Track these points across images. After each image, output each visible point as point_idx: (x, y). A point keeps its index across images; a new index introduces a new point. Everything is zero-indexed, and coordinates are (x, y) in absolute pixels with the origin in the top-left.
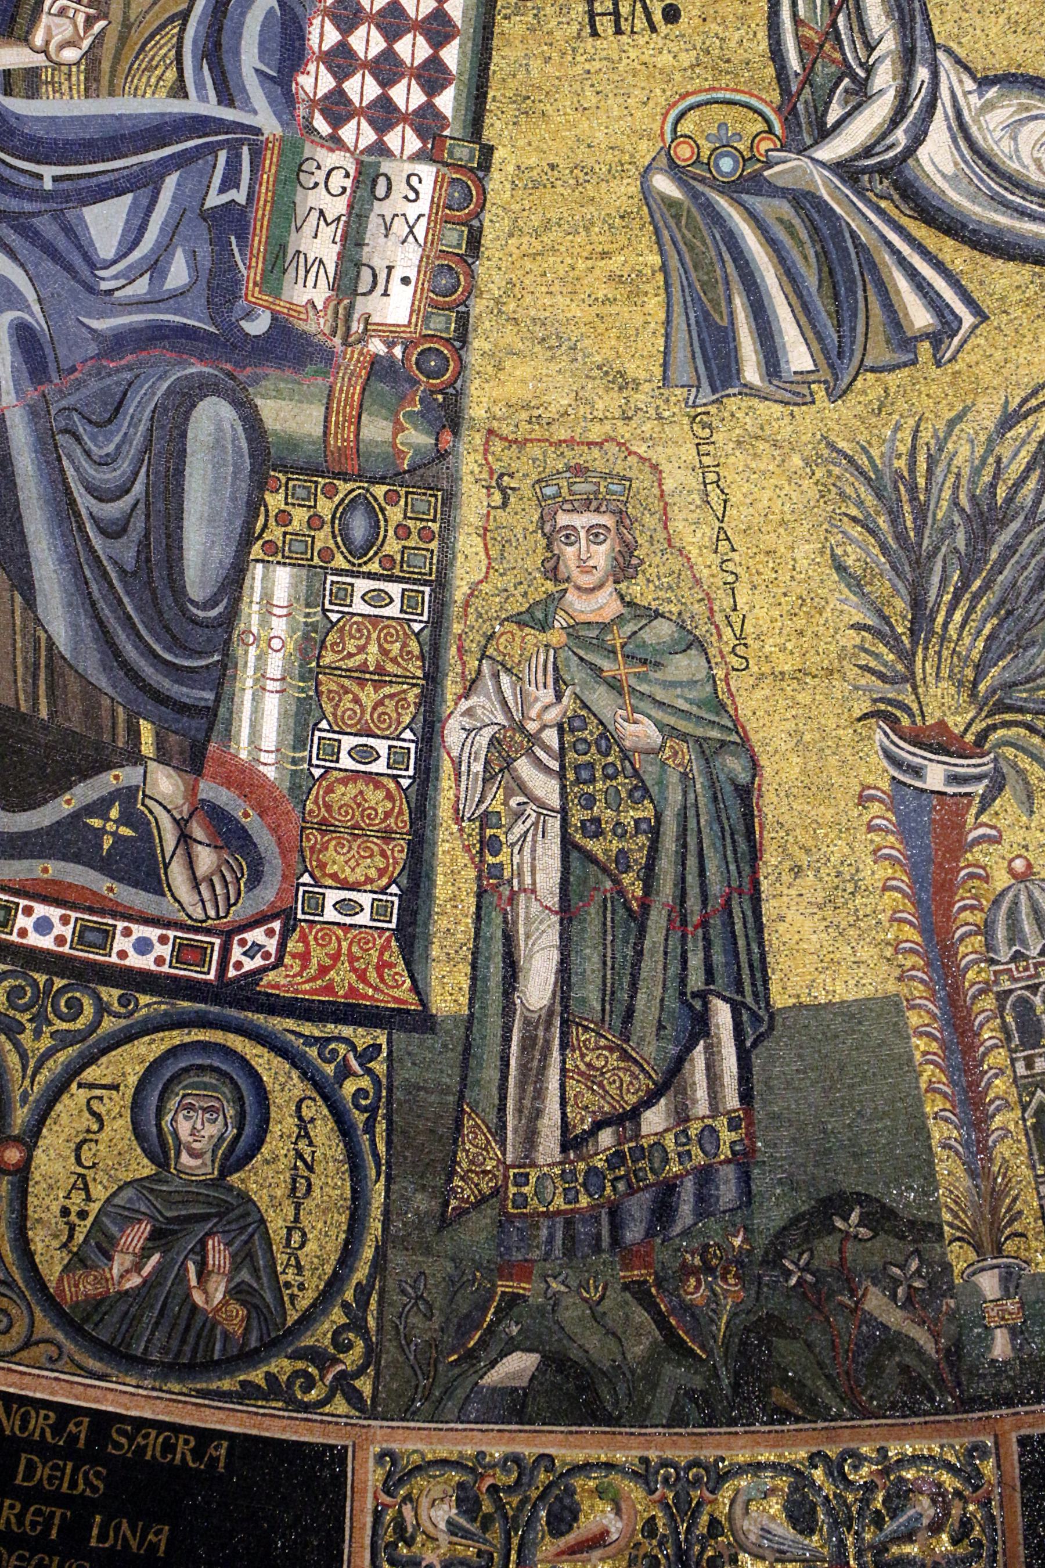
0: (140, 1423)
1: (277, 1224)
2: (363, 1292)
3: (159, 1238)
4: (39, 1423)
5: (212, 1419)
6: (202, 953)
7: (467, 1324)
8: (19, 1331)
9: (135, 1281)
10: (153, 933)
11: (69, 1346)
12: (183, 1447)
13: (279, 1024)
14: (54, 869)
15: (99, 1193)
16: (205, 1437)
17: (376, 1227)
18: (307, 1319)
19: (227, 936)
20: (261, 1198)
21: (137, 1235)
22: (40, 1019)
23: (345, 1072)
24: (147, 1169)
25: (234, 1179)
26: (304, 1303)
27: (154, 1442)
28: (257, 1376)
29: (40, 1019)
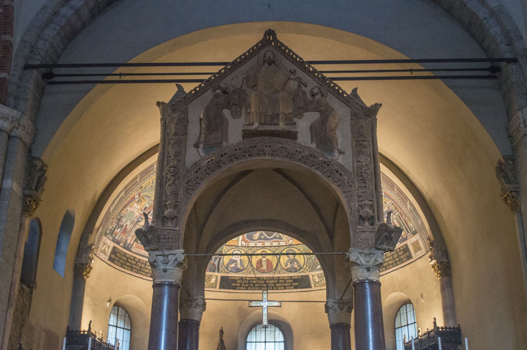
0: (294, 276)
1: (299, 260)
2: (307, 264)
3: (291, 263)
4: (287, 278)
5: (299, 275)
6: (287, 243)
7: (315, 264)
8: (283, 272)
9: (290, 266)
10: (283, 242)
11: (287, 272)
12: (297, 277)
13: (294, 246)
14: (274, 240)
15: (286, 261)
16: (298, 276)
17: (306, 259)
18: (303, 266)
19: (289, 241)
20: (297, 258)
21: (289, 263)
22: (277, 250)
23: (300, 249)
24: (288, 259)
25: (295, 258)
26: (303, 265)
27: (295, 277)
28: (301, 271)
29: (277, 250)
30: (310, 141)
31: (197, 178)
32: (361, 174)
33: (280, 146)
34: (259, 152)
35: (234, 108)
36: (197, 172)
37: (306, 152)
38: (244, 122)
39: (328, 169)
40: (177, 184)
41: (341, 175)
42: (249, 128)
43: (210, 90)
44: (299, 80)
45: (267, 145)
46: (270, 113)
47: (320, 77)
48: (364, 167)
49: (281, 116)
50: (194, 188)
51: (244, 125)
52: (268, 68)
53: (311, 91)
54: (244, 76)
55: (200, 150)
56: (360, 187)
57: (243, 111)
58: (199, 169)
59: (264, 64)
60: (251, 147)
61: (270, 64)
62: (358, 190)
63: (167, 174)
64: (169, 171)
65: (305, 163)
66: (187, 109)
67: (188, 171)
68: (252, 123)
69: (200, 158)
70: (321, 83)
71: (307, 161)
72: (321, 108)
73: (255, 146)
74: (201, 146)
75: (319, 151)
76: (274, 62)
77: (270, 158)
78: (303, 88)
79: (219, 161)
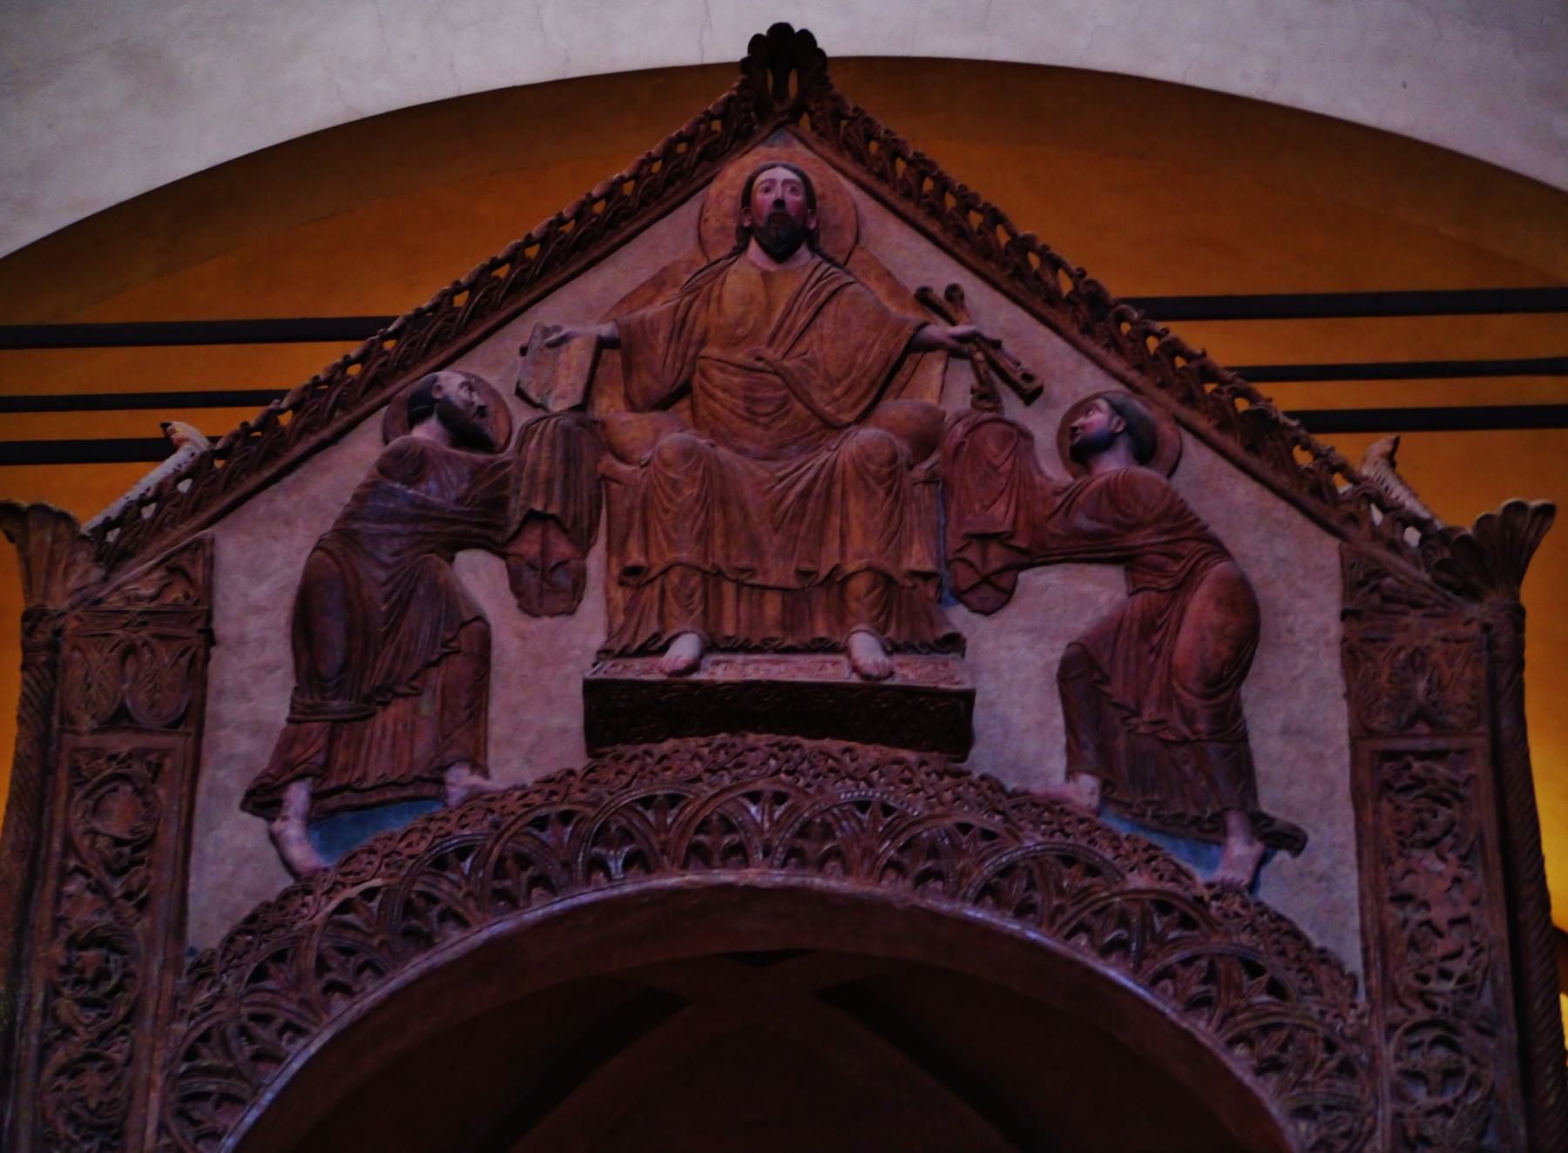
30: (1057, 764)
31: (264, 1019)
32: (1417, 985)
33: (845, 792)
34: (702, 838)
35: (529, 546)
36: (260, 974)
37: (1033, 840)
38: (598, 640)
39: (1186, 954)
40: (119, 1057)
41: (1275, 989)
42: (636, 670)
43: (374, 426)
44: (979, 356)
45: (760, 785)
46: (779, 572)
47: (1128, 336)
48: (1440, 935)
49: (859, 585)
50: (236, 1086)
51: (604, 653)
52: (766, 276)
53: (1067, 430)
54: (606, 330)
55: (292, 829)
56: (1415, 1075)
57: (595, 561)
58: (279, 957)
59: (740, 250)
60: (647, 802)
61: (780, 252)
62: (1398, 1094)
63: (53, 991)
64: (65, 970)
65: (1023, 910)
66: (203, 551)
67: (202, 970)
68: (657, 636)
69: (289, 882)
70: (1133, 375)
71: (1037, 898)
72: (1137, 539)
73: (673, 800)
74: (298, 796)
75: (1123, 830)
76: (811, 239)
77: (777, 877)
78: (1013, 408)
79: (420, 903)
